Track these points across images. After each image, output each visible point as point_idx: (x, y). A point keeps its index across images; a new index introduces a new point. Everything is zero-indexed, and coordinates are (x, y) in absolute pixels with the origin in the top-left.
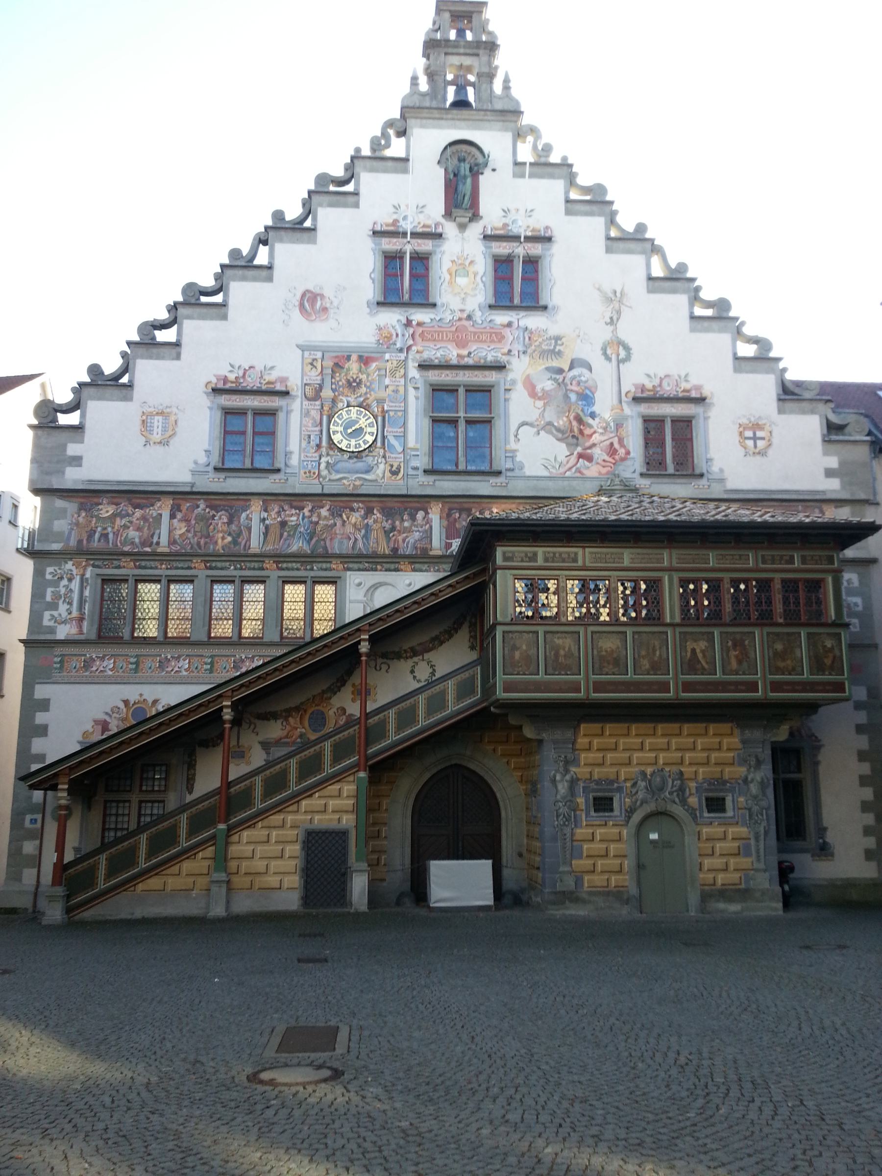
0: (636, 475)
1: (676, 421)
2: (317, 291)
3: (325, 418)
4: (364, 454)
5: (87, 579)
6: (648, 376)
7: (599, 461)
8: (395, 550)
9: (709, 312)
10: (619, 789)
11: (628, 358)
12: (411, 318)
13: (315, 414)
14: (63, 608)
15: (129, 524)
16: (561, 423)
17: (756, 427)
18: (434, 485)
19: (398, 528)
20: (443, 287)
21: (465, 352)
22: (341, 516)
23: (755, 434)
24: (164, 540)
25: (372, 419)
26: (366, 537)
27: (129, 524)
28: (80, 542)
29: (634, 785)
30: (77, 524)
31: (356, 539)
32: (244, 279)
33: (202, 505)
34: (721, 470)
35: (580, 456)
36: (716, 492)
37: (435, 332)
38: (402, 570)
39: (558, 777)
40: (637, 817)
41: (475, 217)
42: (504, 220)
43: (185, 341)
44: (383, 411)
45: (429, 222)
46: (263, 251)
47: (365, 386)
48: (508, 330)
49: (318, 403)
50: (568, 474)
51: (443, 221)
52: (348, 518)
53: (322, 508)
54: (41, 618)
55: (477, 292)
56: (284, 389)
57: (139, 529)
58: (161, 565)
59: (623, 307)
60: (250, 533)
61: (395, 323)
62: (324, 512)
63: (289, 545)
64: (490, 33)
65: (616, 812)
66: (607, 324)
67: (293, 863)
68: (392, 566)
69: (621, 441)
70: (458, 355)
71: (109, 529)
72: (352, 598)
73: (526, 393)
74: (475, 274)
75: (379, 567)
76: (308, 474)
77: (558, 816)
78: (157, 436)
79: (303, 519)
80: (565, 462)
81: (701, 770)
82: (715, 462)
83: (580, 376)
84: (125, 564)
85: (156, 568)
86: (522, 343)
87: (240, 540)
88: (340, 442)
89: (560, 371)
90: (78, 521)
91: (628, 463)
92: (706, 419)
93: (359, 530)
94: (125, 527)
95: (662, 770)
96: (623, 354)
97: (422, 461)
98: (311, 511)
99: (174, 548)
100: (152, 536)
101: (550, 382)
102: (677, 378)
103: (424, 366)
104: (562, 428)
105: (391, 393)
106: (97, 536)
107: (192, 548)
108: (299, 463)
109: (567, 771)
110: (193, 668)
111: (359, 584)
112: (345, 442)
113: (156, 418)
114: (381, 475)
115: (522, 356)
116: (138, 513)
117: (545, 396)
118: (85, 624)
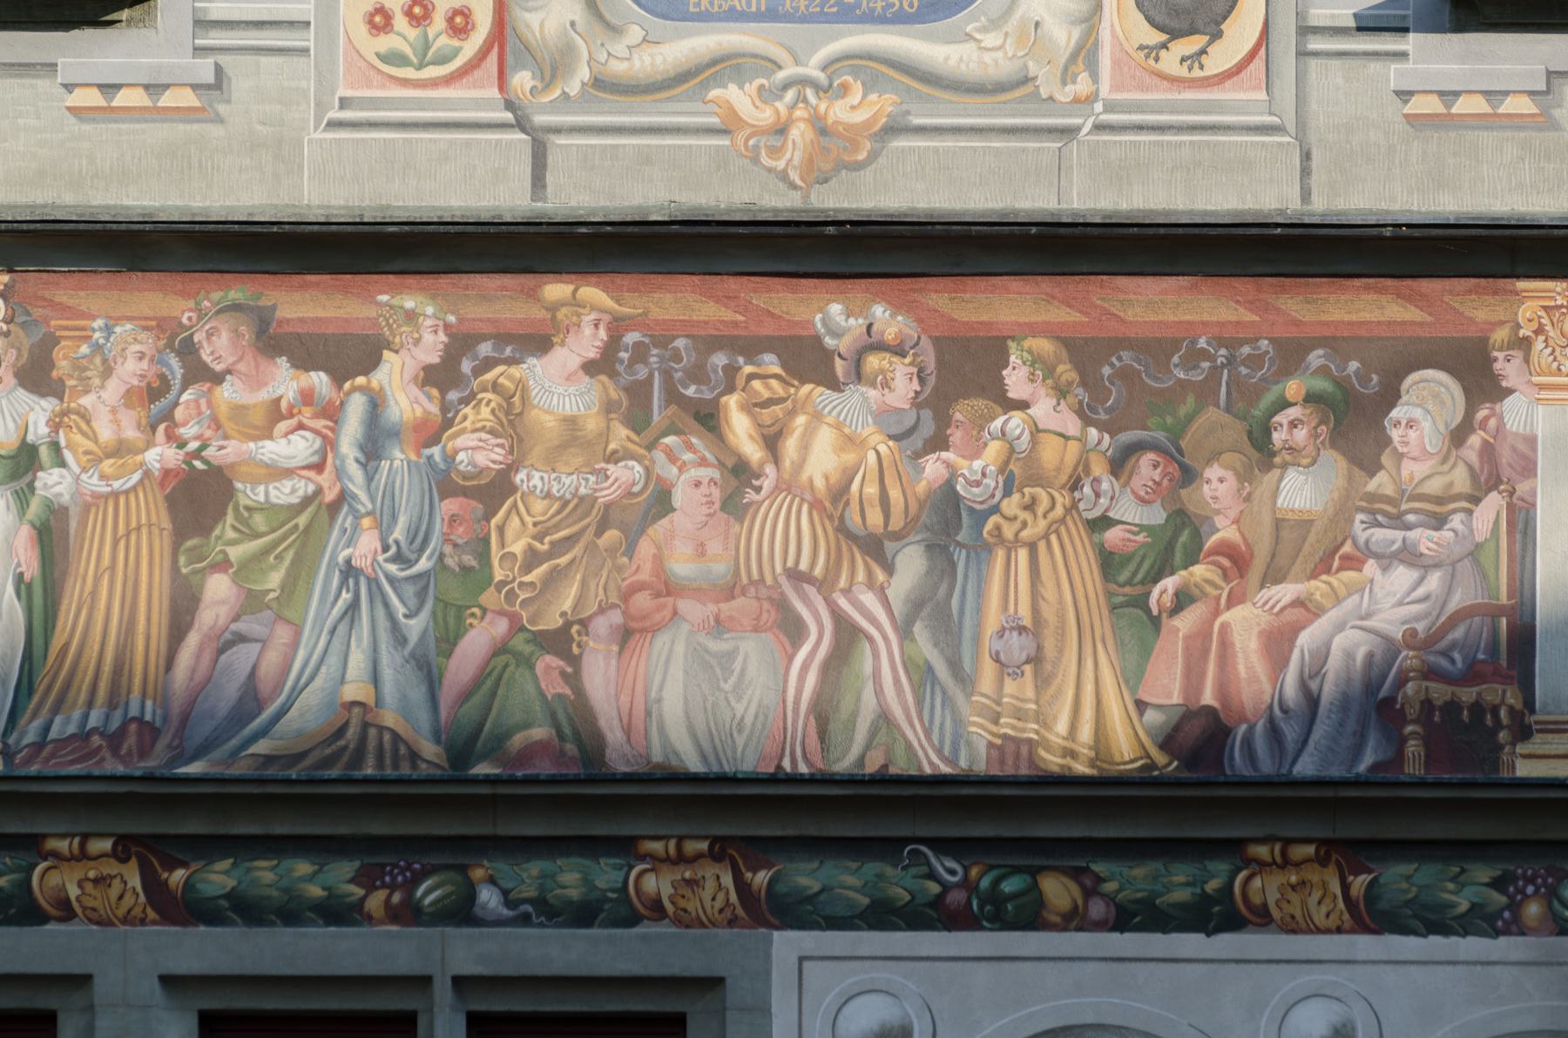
18: (1545, 122)
19: (1225, 531)
22: (708, 419)
31: (847, 635)
38: (1261, 918)
52: (772, 441)
53: (539, 342)
75: (1057, 890)
76: (403, 36)
79: (371, 452)
98: (439, 377)
114: (1063, 37)
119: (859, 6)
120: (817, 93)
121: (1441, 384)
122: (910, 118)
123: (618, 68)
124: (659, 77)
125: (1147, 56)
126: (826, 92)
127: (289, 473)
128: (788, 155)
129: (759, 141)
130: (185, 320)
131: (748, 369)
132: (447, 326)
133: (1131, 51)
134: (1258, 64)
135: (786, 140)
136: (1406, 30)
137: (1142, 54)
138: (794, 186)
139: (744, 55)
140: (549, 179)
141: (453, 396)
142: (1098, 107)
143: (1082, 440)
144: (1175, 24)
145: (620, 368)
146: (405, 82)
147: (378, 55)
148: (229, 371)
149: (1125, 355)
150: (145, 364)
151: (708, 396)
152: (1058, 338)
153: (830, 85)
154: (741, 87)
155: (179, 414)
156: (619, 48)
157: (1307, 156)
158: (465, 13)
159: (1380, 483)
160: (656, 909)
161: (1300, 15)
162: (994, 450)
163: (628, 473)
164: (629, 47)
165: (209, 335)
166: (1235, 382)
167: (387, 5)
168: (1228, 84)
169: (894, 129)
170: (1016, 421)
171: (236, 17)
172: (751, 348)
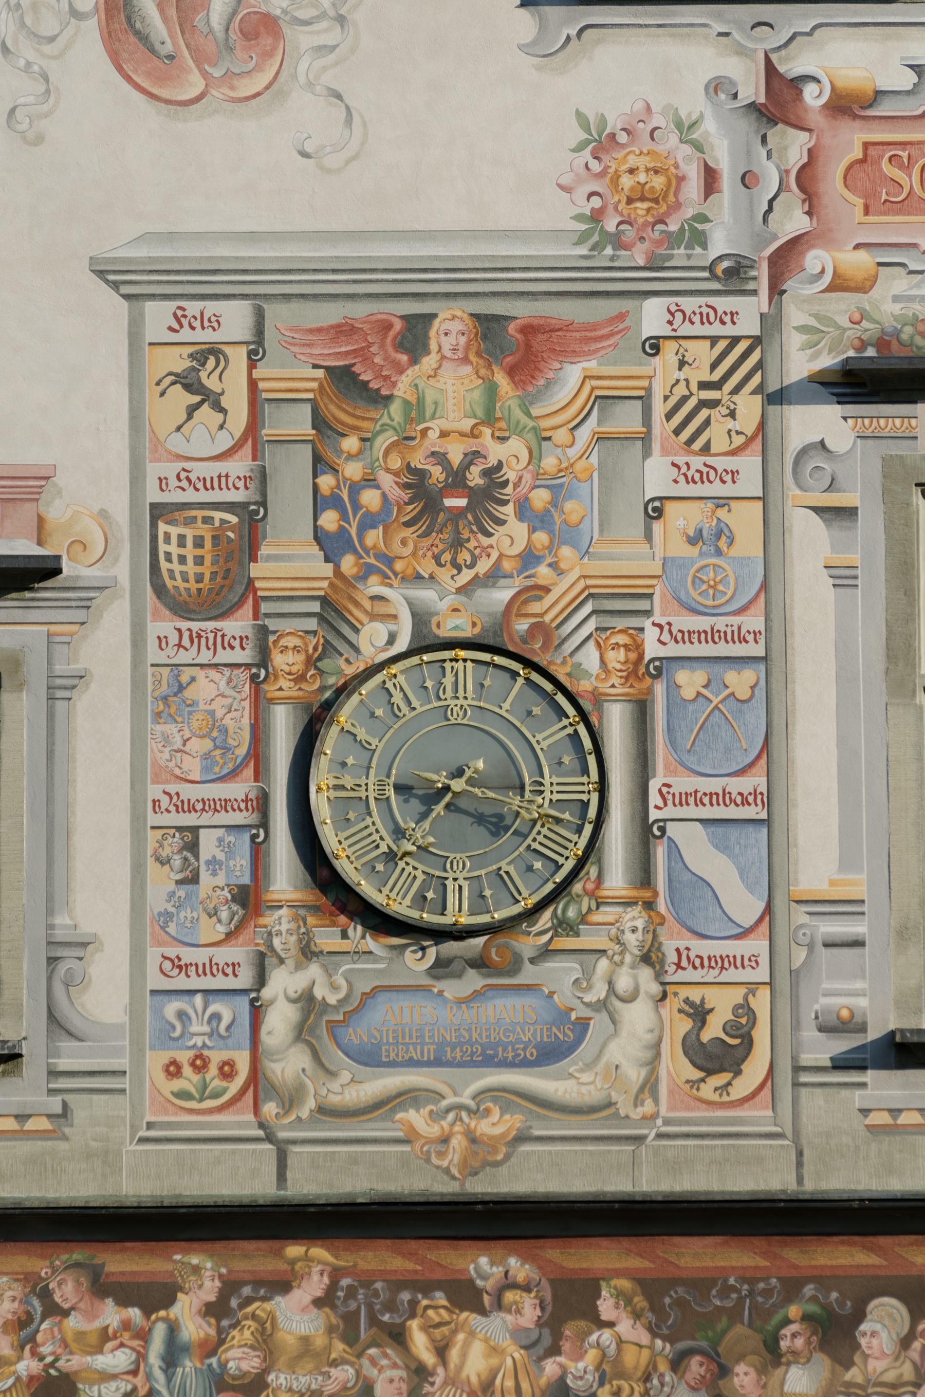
12: (790, 67)
47: (523, 510)
52: (441, 1351)
76: (189, 1080)
79: (170, 1361)
105: (681, 550)
108: (135, 1012)
114: (635, 1075)
119: (497, 1056)
120: (469, 1115)
121: (893, 1307)
122: (532, 1131)
123: (334, 1099)
124: (362, 1105)
125: (692, 1087)
126: (475, 1113)
127: (114, 1377)
128: (450, 1157)
129: (430, 1148)
130: (43, 1274)
131: (425, 1302)
132: (221, 1276)
133: (680, 1084)
134: (766, 1092)
135: (448, 1148)
136: (863, 1068)
137: (688, 1086)
138: (454, 1178)
139: (419, 1090)
140: (289, 1175)
141: (225, 1323)
142: (659, 1122)
143: (651, 1347)
144: (709, 1065)
145: (338, 1303)
146: (191, 1111)
147: (172, 1093)
148: (73, 1308)
149: (681, 1290)
150: (16, 1304)
151: (398, 1321)
152: (634, 1279)
153: (478, 1109)
154: (418, 1111)
155: (40, 1338)
156: (335, 1086)
157: (800, 1154)
158: (230, 1063)
161: (794, 1059)
162: (592, 1355)
163: (344, 1374)
164: (342, 1086)
165: (60, 1284)
166: (754, 1307)
167: (178, 1059)
168: (747, 1105)
169: (522, 1138)
170: (606, 1336)
171: (76, 1068)
172: (427, 1288)
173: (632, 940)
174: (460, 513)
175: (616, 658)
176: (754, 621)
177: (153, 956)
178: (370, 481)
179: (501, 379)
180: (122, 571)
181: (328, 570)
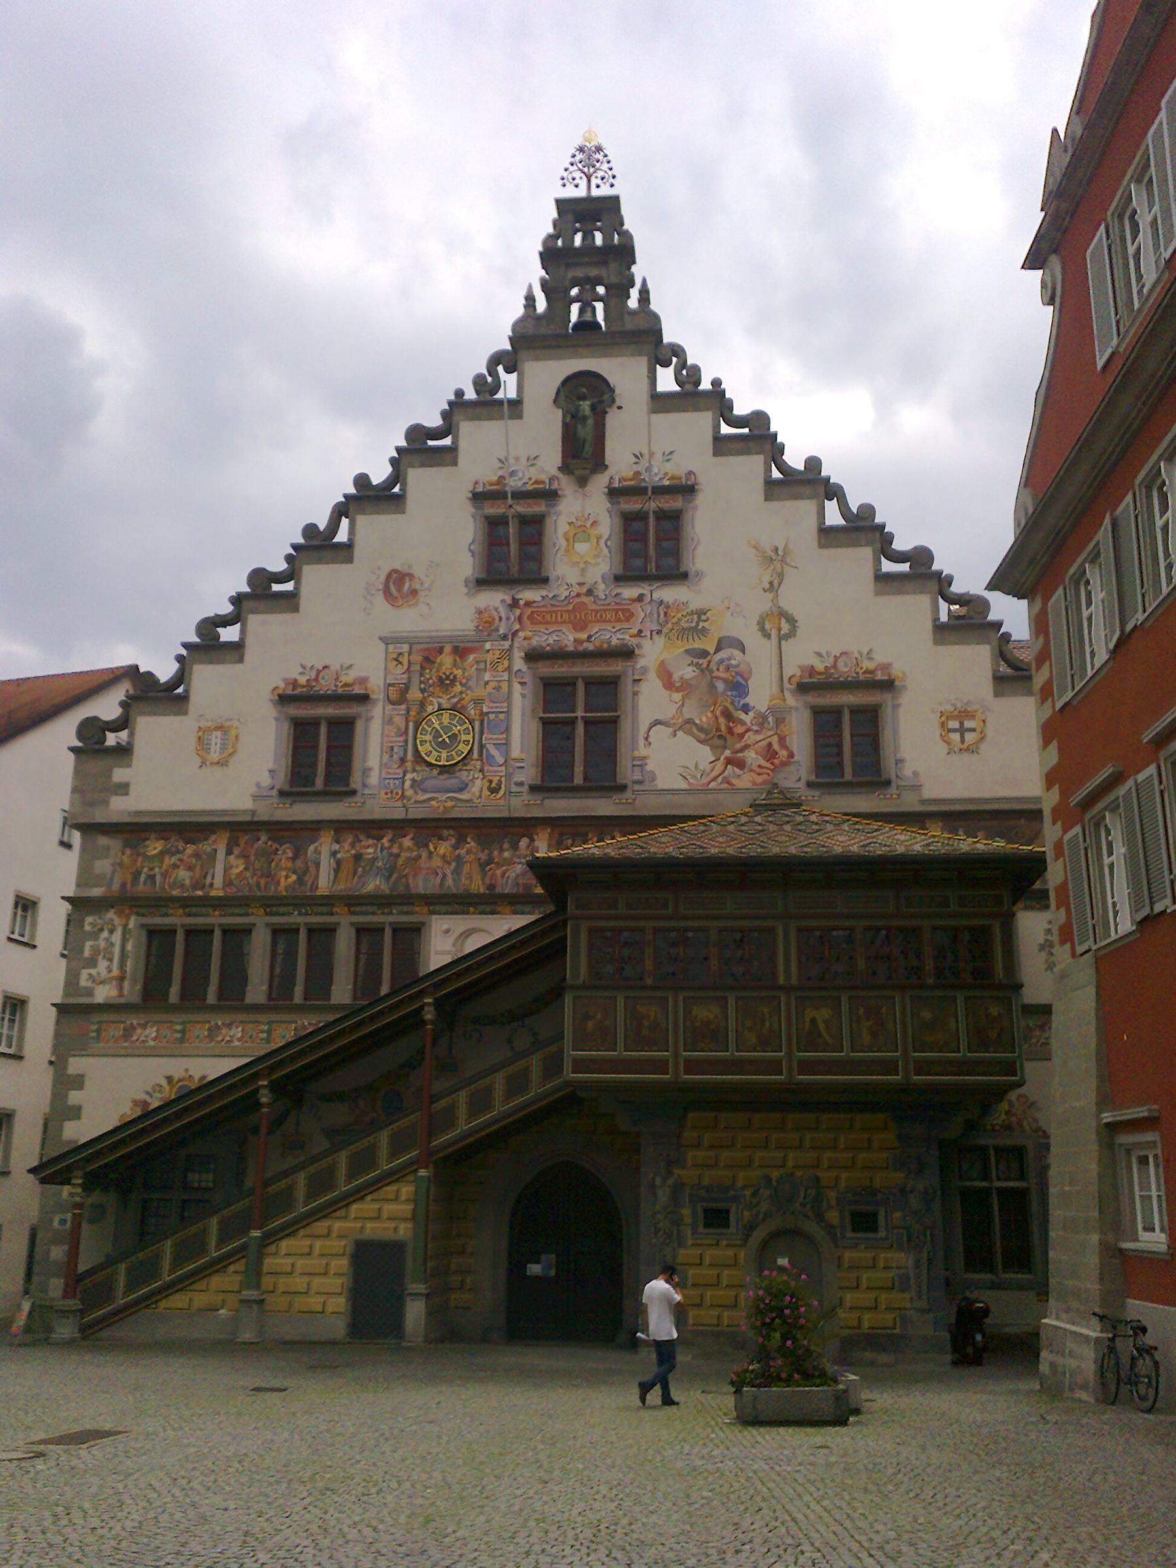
0: (802, 784)
1: (855, 711)
2: (405, 569)
3: (411, 724)
4: (457, 768)
5: (130, 930)
6: (819, 654)
7: (754, 767)
8: (491, 887)
9: (905, 567)
10: (735, 1199)
11: (792, 634)
12: (516, 597)
13: (399, 721)
14: (102, 965)
15: (178, 863)
16: (704, 719)
17: (964, 714)
18: (542, 804)
20: (559, 555)
21: (584, 636)
22: (427, 846)
23: (962, 724)
24: (218, 881)
25: (468, 725)
26: (457, 872)
27: (178, 863)
28: (124, 885)
29: (754, 1194)
30: (121, 864)
31: (445, 875)
32: (319, 561)
33: (264, 838)
34: (916, 774)
35: (729, 761)
36: (910, 803)
37: (547, 612)
39: (658, 1181)
40: (759, 1234)
41: (599, 463)
42: (636, 468)
43: (249, 641)
44: (482, 714)
45: (543, 477)
46: (345, 522)
47: (461, 684)
48: (638, 605)
49: (403, 707)
50: (713, 785)
51: (560, 475)
52: (435, 849)
53: (405, 836)
54: (77, 976)
55: (600, 560)
56: (363, 692)
57: (190, 868)
58: (214, 910)
59: (786, 568)
60: (318, 871)
61: (498, 604)
62: (407, 842)
63: (363, 885)
64: (627, 237)
65: (732, 1229)
66: (765, 591)
67: (339, 1281)
68: (488, 909)
69: (782, 740)
70: (575, 640)
71: (157, 870)
72: (439, 949)
73: (661, 685)
74: (599, 538)
75: (472, 909)
76: (389, 795)
77: (656, 1234)
78: (214, 755)
79: (382, 850)
80: (708, 770)
81: (844, 1176)
82: (907, 765)
83: (729, 659)
84: (171, 911)
85: (207, 915)
86: (655, 621)
87: (306, 878)
88: (429, 754)
89: (704, 654)
90: (122, 861)
91: (792, 768)
92: (896, 707)
93: (449, 863)
94: (176, 866)
95: (792, 1174)
96: (785, 627)
97: (529, 774)
99: (232, 891)
100: (205, 877)
101: (691, 668)
102: (857, 655)
103: (532, 656)
104: (705, 726)
106: (142, 878)
107: (250, 889)
108: (380, 782)
109: (670, 1173)
110: (247, 1038)
111: (447, 931)
112: (435, 753)
113: (215, 733)
114: (477, 794)
115: (655, 637)
116: (190, 849)
117: (685, 687)
118: (126, 984)
159: (518, 853)
160: (417, 913)
162: (465, 850)
163: (415, 853)
173: (478, 767)
174: (447, 684)
175: (477, 712)
176: (506, 704)
177: (384, 771)
178: (431, 678)
179: (458, 658)
180: (381, 697)
181: (421, 695)
